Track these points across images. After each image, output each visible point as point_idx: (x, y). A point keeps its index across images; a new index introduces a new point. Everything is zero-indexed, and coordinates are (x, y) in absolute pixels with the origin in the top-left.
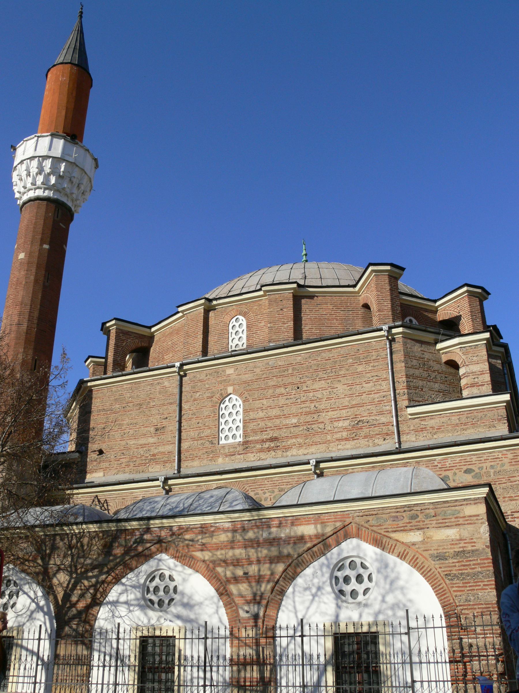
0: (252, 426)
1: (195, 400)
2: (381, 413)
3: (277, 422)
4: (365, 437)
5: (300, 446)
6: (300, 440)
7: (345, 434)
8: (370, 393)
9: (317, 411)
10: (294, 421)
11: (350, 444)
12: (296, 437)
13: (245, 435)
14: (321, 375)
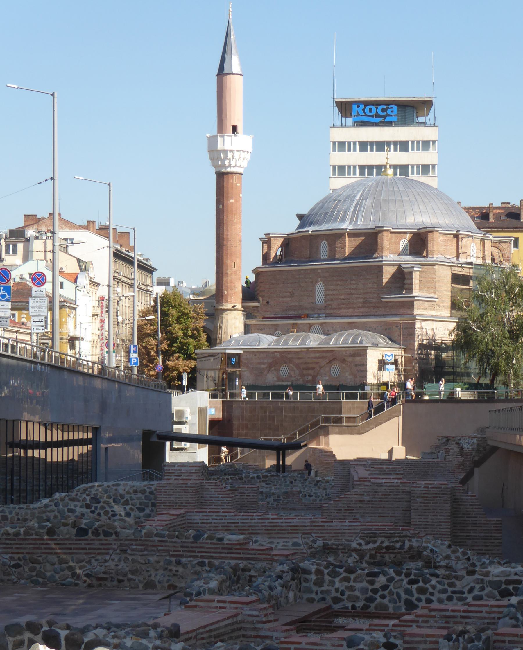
0: (328, 297)
1: (306, 282)
2: (373, 298)
3: (337, 297)
4: (367, 307)
5: (345, 308)
6: (345, 306)
7: (361, 305)
8: (370, 288)
9: (352, 294)
10: (343, 297)
11: (362, 310)
12: (343, 304)
13: (325, 302)
14: (354, 278)
